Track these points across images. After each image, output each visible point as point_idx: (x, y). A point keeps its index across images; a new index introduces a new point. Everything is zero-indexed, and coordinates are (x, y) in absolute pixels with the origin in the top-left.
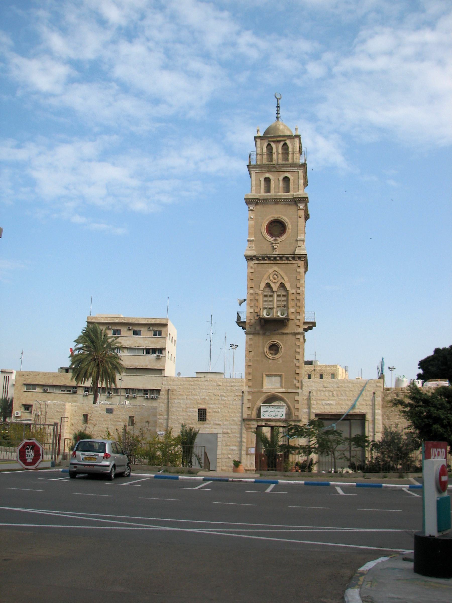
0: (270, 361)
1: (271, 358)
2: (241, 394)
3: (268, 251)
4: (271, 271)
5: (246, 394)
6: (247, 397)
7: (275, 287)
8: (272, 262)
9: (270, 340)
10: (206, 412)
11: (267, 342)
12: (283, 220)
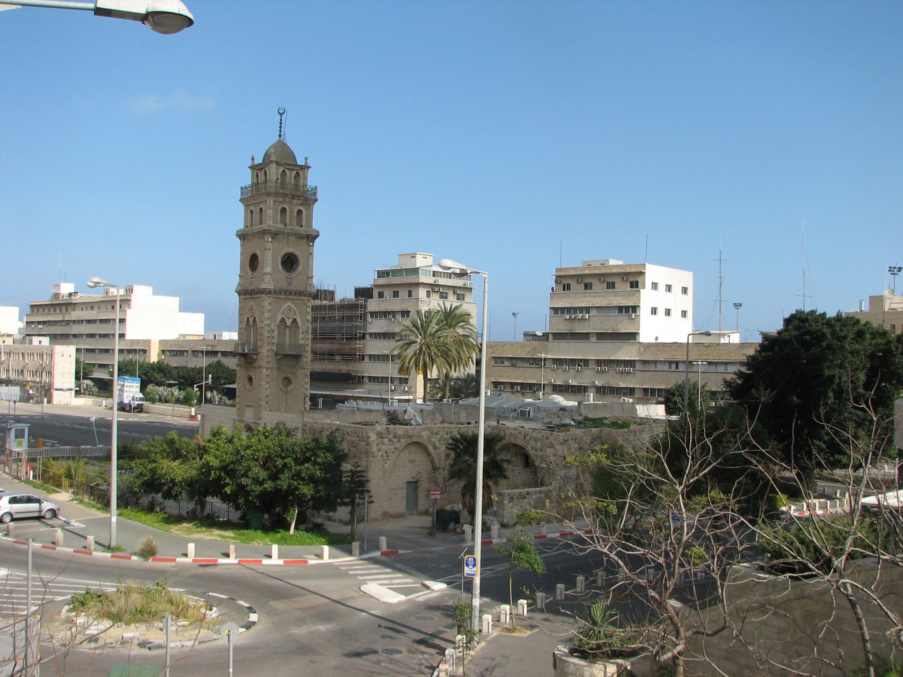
3: (284, 285)
4: (286, 306)
7: (289, 322)
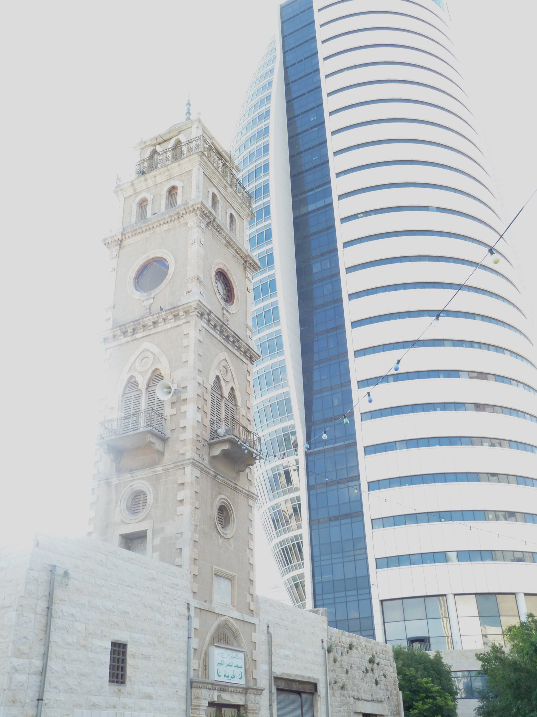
0: (221, 540)
1: (222, 534)
2: (185, 612)
5: (192, 612)
6: (196, 623)
8: (223, 341)
9: (220, 494)
10: (124, 653)
11: (216, 496)
12: (232, 280)
